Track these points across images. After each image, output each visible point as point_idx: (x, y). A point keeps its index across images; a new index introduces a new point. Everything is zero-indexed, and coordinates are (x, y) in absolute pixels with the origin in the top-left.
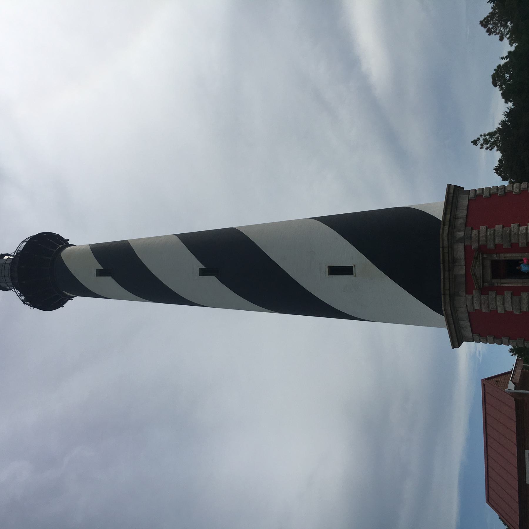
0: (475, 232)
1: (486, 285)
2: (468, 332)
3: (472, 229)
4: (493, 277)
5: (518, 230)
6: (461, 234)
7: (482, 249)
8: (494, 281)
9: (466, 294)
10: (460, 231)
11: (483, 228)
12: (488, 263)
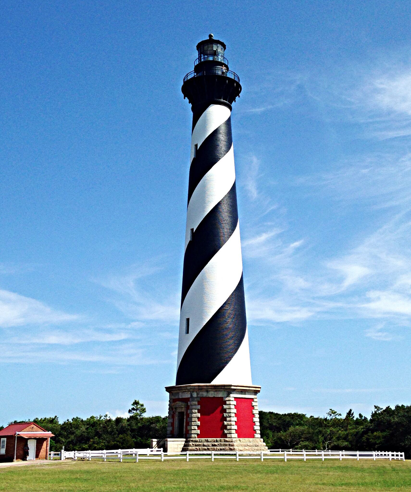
0: (196, 403)
1: (174, 410)
2: (173, 397)
3: (198, 402)
4: (179, 413)
5: (195, 425)
6: (195, 395)
7: (188, 407)
8: (177, 413)
9: (173, 399)
10: (197, 394)
11: (199, 407)
12: (183, 411)
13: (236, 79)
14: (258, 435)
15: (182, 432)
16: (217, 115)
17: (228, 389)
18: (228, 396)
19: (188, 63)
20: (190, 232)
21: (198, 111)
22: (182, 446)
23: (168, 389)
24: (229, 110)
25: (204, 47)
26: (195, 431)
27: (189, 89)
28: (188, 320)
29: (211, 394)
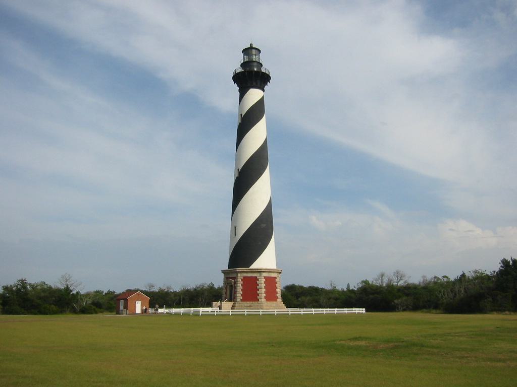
8: (228, 287)
13: (267, 73)
14: (280, 300)
15: (232, 298)
16: (254, 95)
17: (259, 271)
18: (260, 276)
19: (235, 64)
20: (237, 170)
21: (243, 92)
22: (231, 306)
23: (223, 272)
24: (262, 92)
25: (246, 51)
26: (239, 296)
27: (237, 78)
28: (236, 227)
29: (249, 275)
